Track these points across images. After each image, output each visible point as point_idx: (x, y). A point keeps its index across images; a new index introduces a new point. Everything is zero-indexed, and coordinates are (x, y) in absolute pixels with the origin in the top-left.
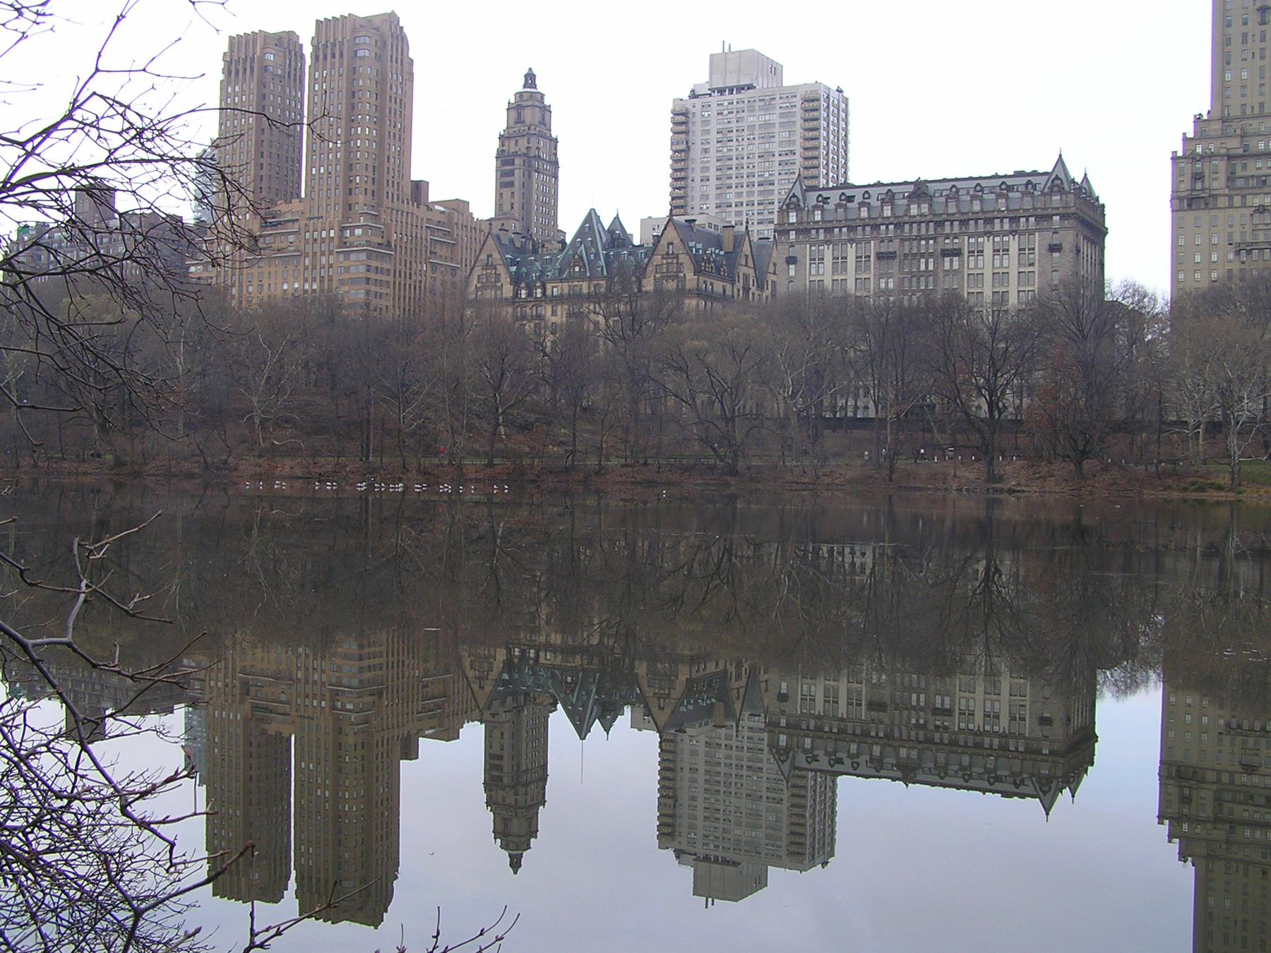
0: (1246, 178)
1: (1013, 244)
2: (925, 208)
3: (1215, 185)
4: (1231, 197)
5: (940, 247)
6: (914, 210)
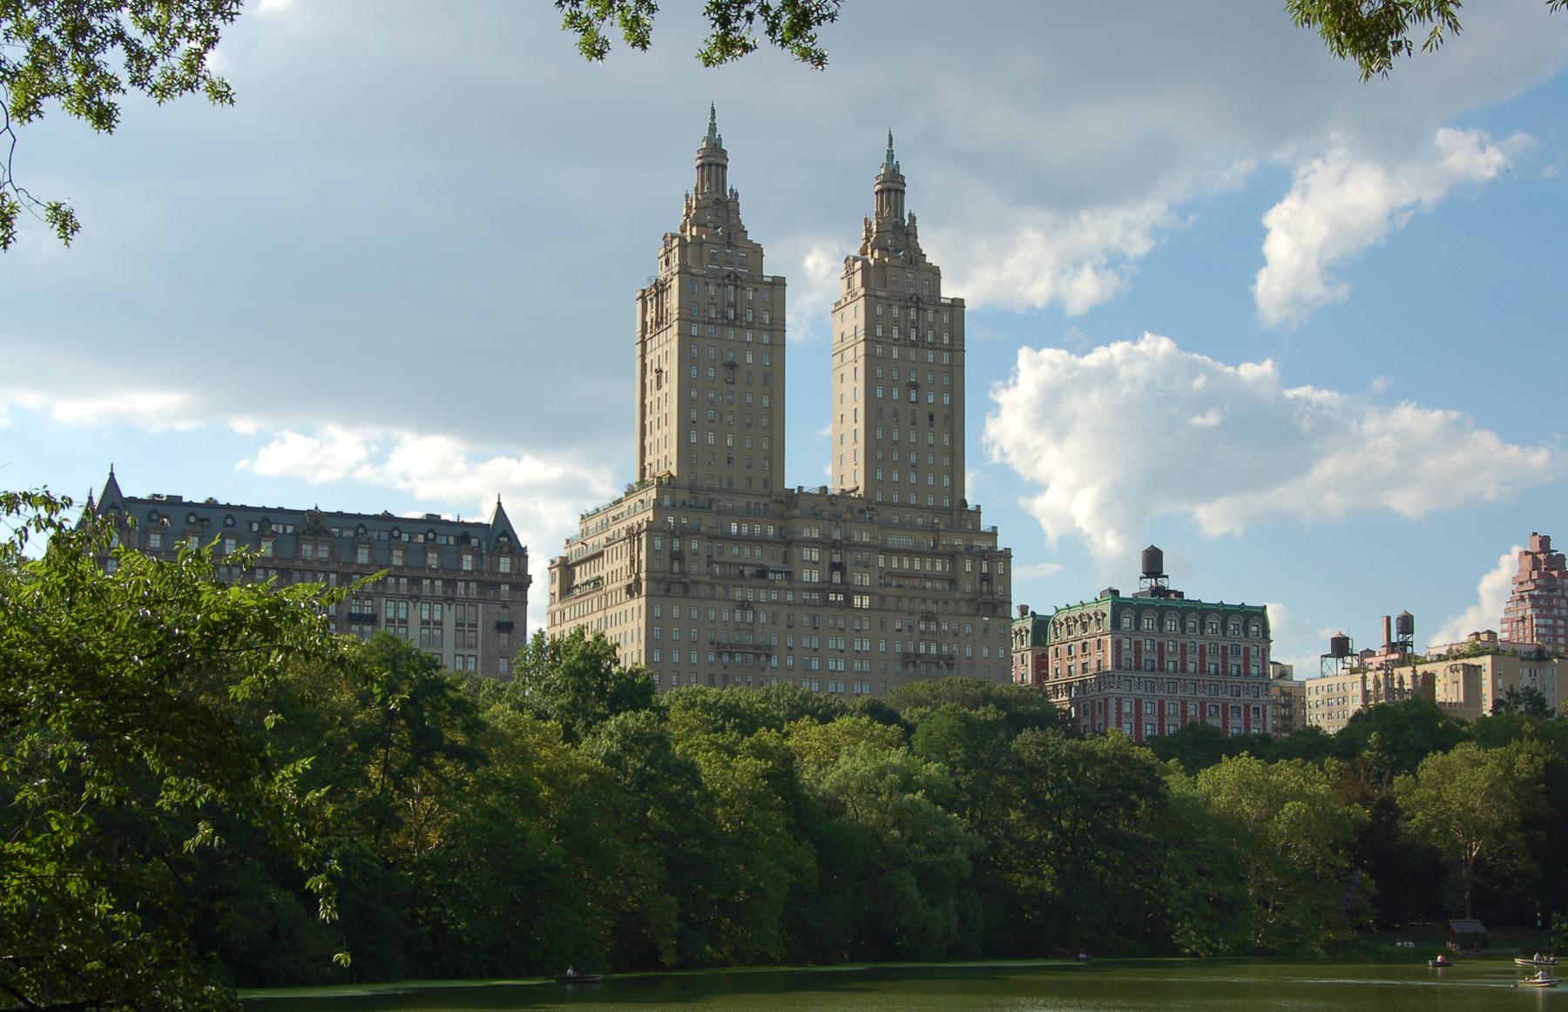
0: (722, 564)
1: (450, 616)
2: (324, 553)
3: (694, 568)
4: (712, 586)
5: (345, 610)
6: (307, 550)
